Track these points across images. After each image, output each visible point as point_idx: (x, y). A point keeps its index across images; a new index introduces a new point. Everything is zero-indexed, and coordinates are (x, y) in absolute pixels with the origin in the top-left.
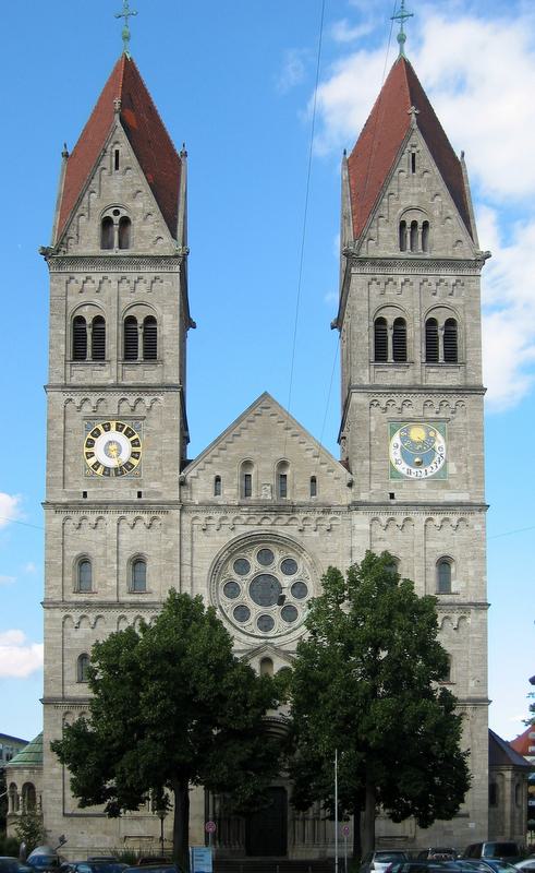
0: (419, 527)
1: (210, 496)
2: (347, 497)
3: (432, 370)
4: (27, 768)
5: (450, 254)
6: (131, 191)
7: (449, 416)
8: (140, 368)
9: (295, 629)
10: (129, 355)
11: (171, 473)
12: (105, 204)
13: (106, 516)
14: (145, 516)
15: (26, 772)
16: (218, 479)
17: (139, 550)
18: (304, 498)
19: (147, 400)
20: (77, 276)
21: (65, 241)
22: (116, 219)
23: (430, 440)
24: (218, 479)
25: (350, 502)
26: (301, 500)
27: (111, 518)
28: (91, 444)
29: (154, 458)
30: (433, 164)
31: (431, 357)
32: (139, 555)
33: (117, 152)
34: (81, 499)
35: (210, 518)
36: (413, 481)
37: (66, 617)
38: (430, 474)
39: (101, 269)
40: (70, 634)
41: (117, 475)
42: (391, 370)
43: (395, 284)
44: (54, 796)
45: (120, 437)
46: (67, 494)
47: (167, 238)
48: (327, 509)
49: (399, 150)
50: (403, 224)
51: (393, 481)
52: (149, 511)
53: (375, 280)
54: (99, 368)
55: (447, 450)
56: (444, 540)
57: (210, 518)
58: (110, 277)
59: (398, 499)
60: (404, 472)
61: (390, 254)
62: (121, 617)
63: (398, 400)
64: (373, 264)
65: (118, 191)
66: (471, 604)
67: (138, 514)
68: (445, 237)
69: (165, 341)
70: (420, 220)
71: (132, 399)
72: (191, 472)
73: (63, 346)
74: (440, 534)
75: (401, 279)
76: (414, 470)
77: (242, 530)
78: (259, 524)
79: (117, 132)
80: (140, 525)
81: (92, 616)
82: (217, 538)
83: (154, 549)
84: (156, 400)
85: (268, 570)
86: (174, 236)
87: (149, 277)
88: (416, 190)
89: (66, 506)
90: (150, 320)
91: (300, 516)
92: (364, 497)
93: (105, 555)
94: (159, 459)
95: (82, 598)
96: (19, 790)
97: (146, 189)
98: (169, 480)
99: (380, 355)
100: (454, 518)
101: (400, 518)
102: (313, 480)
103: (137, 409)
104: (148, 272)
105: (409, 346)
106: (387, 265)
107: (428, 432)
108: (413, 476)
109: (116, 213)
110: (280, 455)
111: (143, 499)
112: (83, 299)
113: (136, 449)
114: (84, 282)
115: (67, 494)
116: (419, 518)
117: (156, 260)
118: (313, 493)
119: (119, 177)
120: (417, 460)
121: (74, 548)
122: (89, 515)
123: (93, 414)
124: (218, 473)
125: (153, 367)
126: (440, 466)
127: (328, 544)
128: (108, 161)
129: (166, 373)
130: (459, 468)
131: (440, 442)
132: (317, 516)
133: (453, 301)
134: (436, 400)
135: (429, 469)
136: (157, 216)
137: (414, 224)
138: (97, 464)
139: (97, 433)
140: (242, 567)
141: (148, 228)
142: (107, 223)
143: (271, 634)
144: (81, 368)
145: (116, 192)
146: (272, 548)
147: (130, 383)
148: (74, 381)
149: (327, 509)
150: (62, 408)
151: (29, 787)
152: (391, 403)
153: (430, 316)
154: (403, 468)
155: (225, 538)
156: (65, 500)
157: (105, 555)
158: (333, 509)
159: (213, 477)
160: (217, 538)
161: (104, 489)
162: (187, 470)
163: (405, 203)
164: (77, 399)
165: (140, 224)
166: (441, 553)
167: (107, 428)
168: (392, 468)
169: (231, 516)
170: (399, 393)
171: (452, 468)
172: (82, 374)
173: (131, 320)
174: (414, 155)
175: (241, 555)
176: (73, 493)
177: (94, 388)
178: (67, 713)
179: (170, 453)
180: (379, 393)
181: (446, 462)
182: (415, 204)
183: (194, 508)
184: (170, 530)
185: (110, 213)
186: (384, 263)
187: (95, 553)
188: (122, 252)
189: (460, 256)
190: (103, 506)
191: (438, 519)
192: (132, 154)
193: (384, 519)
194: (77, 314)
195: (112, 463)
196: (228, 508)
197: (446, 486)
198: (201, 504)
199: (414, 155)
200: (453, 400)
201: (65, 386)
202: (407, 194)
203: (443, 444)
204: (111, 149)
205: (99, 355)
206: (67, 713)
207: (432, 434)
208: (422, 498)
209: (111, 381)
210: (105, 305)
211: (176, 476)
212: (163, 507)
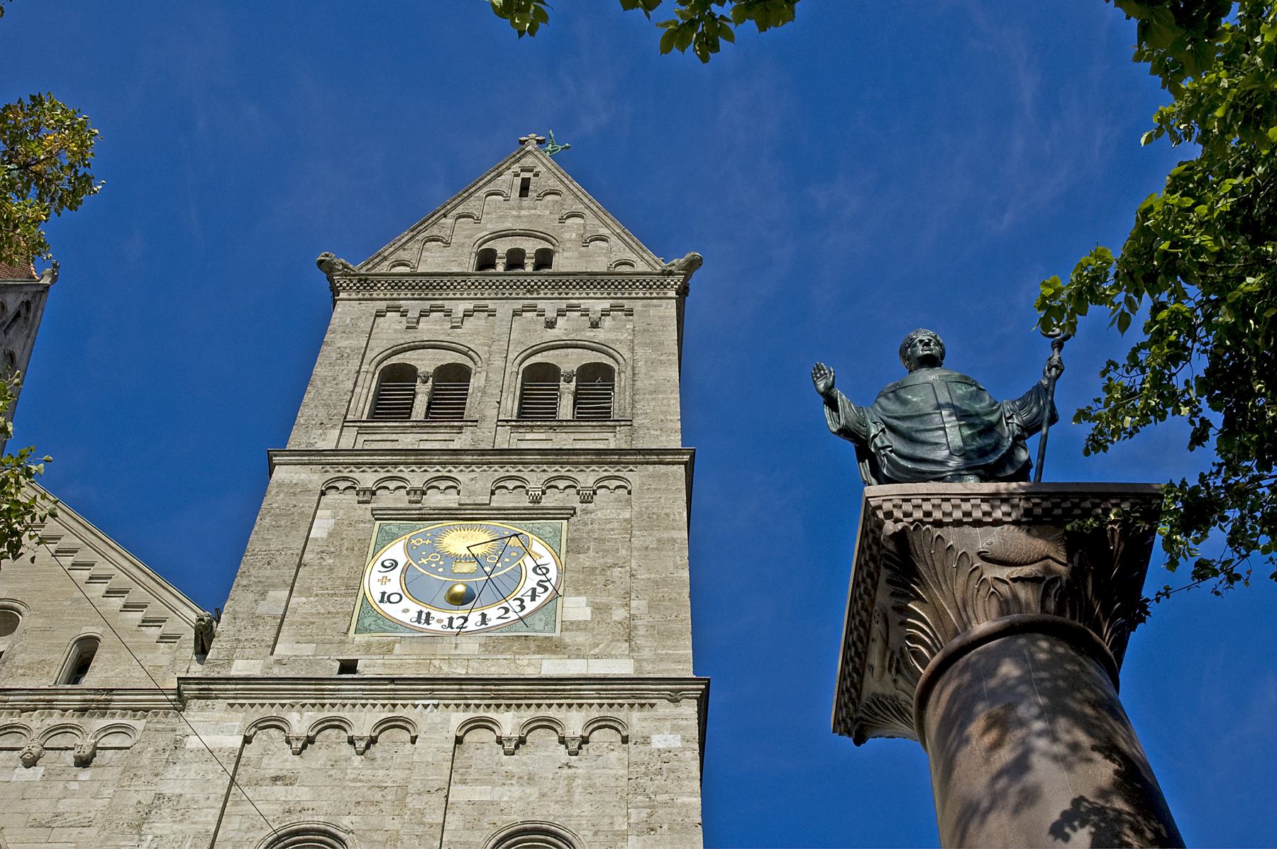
101: (364, 721)
108: (434, 626)
137: (515, 260)
181: (556, 595)
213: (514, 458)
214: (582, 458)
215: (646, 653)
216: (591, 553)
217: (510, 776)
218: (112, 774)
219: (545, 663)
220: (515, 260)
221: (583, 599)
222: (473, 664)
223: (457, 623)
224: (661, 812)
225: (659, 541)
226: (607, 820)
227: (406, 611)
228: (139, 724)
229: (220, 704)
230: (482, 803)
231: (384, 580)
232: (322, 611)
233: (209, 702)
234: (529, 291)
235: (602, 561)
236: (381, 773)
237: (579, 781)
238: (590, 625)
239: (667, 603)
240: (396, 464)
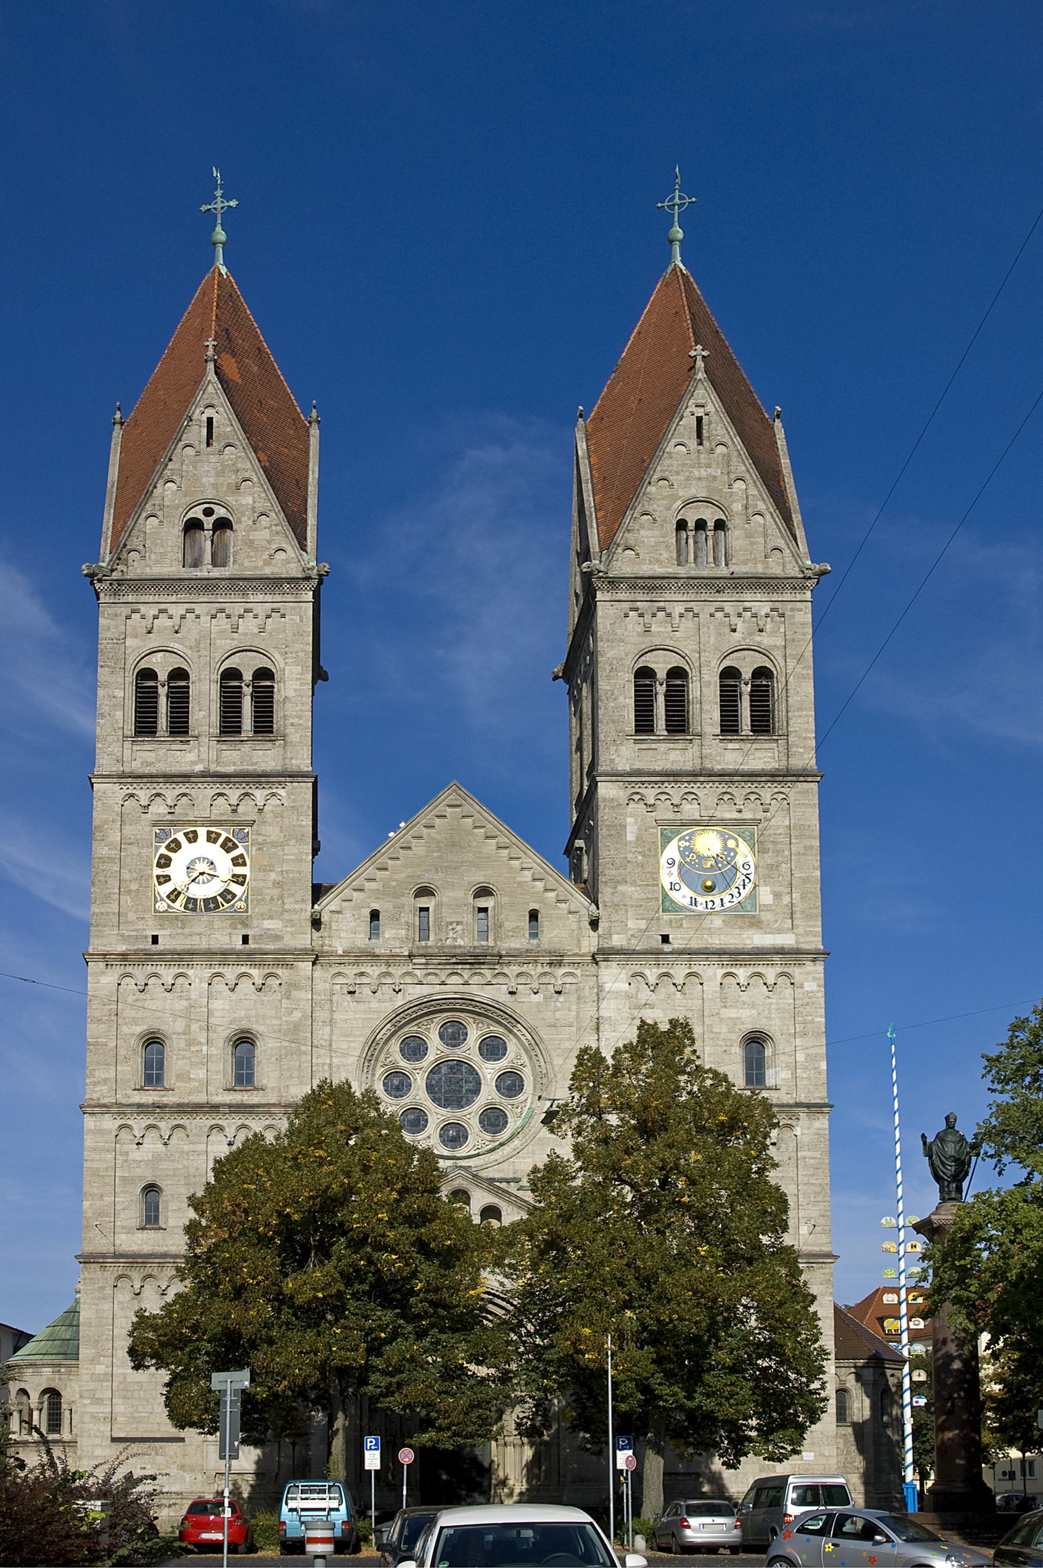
0: (711, 987)
1: (361, 940)
2: (590, 942)
3: (730, 746)
4: (48, 1365)
5: (760, 569)
6: (233, 479)
7: (760, 815)
8: (246, 748)
9: (502, 1145)
10: (230, 725)
11: (297, 907)
12: (188, 500)
13: (190, 972)
14: (254, 972)
15: (47, 1371)
16: (375, 915)
17: (245, 1025)
18: (518, 942)
19: (260, 795)
20: (143, 609)
21: (124, 555)
22: (208, 522)
23: (729, 853)
24: (375, 915)
25: (594, 950)
26: (513, 945)
27: (198, 974)
28: (165, 862)
29: (270, 885)
30: (732, 431)
31: (729, 726)
32: (243, 1031)
33: (210, 421)
34: (149, 945)
35: (362, 974)
36: (700, 916)
37: (121, 1127)
38: (727, 905)
39: (182, 597)
40: (127, 1153)
41: (207, 909)
42: (663, 747)
43: (669, 615)
44: (94, 1409)
45: (215, 852)
47: (292, 550)
48: (557, 960)
49: (672, 409)
50: (681, 525)
51: (666, 917)
52: (261, 964)
53: (636, 609)
54: (179, 747)
55: (756, 867)
56: (753, 1005)
57: (362, 974)
58: (199, 609)
59: (677, 942)
60: (686, 902)
61: (659, 570)
62: (212, 1128)
63: (676, 792)
64: (633, 587)
65: (212, 480)
66: (798, 1105)
67: (243, 969)
68: (752, 543)
69: (288, 706)
70: (711, 516)
71: (234, 794)
72: (329, 904)
73: (119, 714)
74: (744, 997)
75: (679, 608)
76: (701, 900)
77: (415, 992)
78: (443, 983)
79: (210, 389)
80: (245, 985)
81: (165, 1126)
82: (374, 1005)
83: (268, 1022)
84: (274, 795)
85: (458, 1053)
86: (303, 547)
87: (261, 610)
88: (703, 473)
89: (124, 957)
90: (264, 674)
91: (512, 970)
92: (617, 941)
93: (187, 1031)
94: (277, 884)
95: (150, 1097)
96: (35, 1397)
97: (257, 476)
98: (295, 917)
99: (644, 725)
100: (771, 973)
101: (679, 972)
102: (534, 916)
103: (240, 809)
104: (261, 601)
105: (694, 709)
106: (654, 588)
107: (725, 841)
108: (700, 908)
109: (208, 512)
110: (479, 878)
111: (252, 945)
112: (154, 641)
113: (239, 870)
114: (156, 617)
115: (124, 938)
116: (713, 972)
117: (274, 583)
118: (534, 935)
119: (213, 459)
120: (709, 883)
121: (135, 1021)
122: (161, 970)
123: (169, 817)
124: (376, 906)
125: (269, 745)
126: (744, 893)
127: (558, 1015)
128: (197, 433)
129: (289, 755)
130: (777, 895)
131: (744, 854)
132: (540, 969)
133: (765, 640)
134: (739, 792)
135: (727, 898)
136: (276, 518)
137: (701, 525)
139: (175, 846)
141: (261, 535)
142: (193, 526)
143: (462, 1152)
144: (148, 747)
145: (208, 480)
146: (466, 1018)
147: (231, 769)
148: (136, 767)
149: (557, 960)
150: (118, 809)
151: (53, 1394)
152: (663, 797)
153: (727, 663)
154: (682, 896)
155: (388, 1004)
156: (122, 948)
157: (187, 1031)
158: (566, 960)
159: (366, 913)
160: (374, 1005)
161: (187, 931)
162: (325, 901)
163: (685, 493)
164: (143, 795)
165: (250, 529)
166: (748, 1027)
167: (192, 838)
168: (665, 896)
169: (397, 971)
170: (676, 782)
171: (765, 896)
172: (151, 757)
173: (232, 674)
174: (699, 420)
175: (411, 1029)
177: (170, 778)
178: (120, 1277)
179: (297, 875)
180: (643, 782)
182: (702, 494)
183: (338, 960)
184: (295, 994)
185: (197, 513)
186: (652, 584)
187: (172, 1027)
188: (216, 573)
189: (777, 571)
190: (183, 957)
191: (742, 973)
192: (237, 425)
193: (652, 974)
194: (143, 665)
195: (202, 891)
196: (391, 959)
197: (756, 923)
198: (346, 953)
199: (699, 420)
200: (767, 792)
201: (122, 776)
202: (688, 479)
203: (751, 859)
204: (201, 416)
205: (180, 726)
206: (120, 1277)
207: (731, 844)
208: (716, 942)
209: (199, 768)
210: (189, 652)
211: (307, 909)
212: (285, 957)
213: (727, 779)
214: (763, 779)
215: (801, 930)
216: (770, 854)
217: (744, 1003)
218: (573, 998)
219: (755, 936)
220: (701, 525)
221: (768, 888)
222: (722, 937)
223: (710, 905)
224: (809, 1026)
225: (805, 847)
226: (786, 1028)
227: (684, 897)
228: (578, 972)
229: (614, 964)
230: (734, 1019)
231: (670, 874)
232: (644, 897)
233: (609, 963)
234: (718, 591)
235: (776, 859)
236: (690, 1001)
237: (773, 1006)
238: (773, 907)
239: (810, 896)
240: (663, 782)
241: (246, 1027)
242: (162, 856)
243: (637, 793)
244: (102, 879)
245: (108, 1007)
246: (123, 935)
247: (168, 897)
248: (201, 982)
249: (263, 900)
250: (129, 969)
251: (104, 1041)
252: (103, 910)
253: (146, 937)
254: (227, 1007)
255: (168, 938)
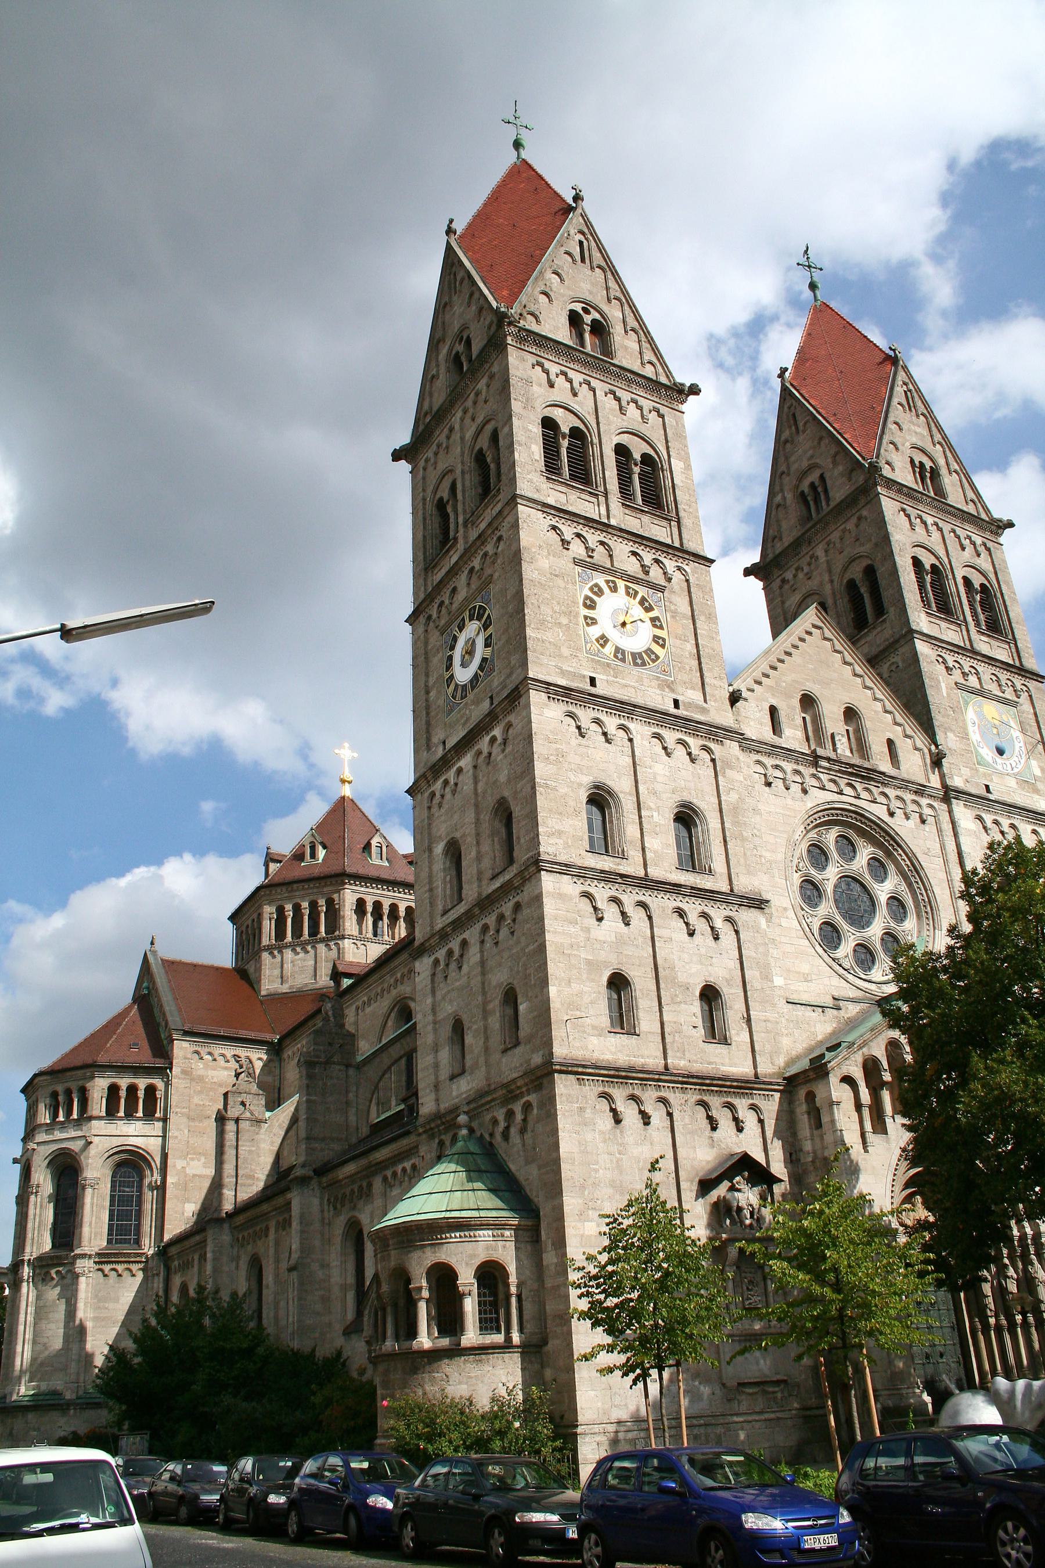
16: (773, 711)
19: (670, 565)
34: (587, 687)
46: (563, 673)
78: (841, 793)
95: (606, 863)
121: (579, 769)
138: (603, 640)
140: (848, 848)
148: (551, 501)
176: (574, 674)
185: (578, 307)
241: (688, 800)
242: (587, 597)
243: (893, 663)
244: (535, 602)
245: (554, 746)
246: (560, 668)
247: (597, 640)
248: (642, 739)
249: (684, 668)
250: (572, 708)
251: (554, 784)
252: (539, 636)
253: (584, 677)
254: (667, 774)
255: (605, 683)
